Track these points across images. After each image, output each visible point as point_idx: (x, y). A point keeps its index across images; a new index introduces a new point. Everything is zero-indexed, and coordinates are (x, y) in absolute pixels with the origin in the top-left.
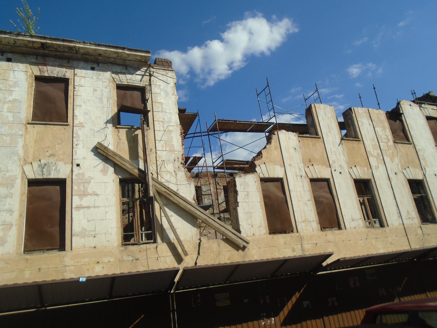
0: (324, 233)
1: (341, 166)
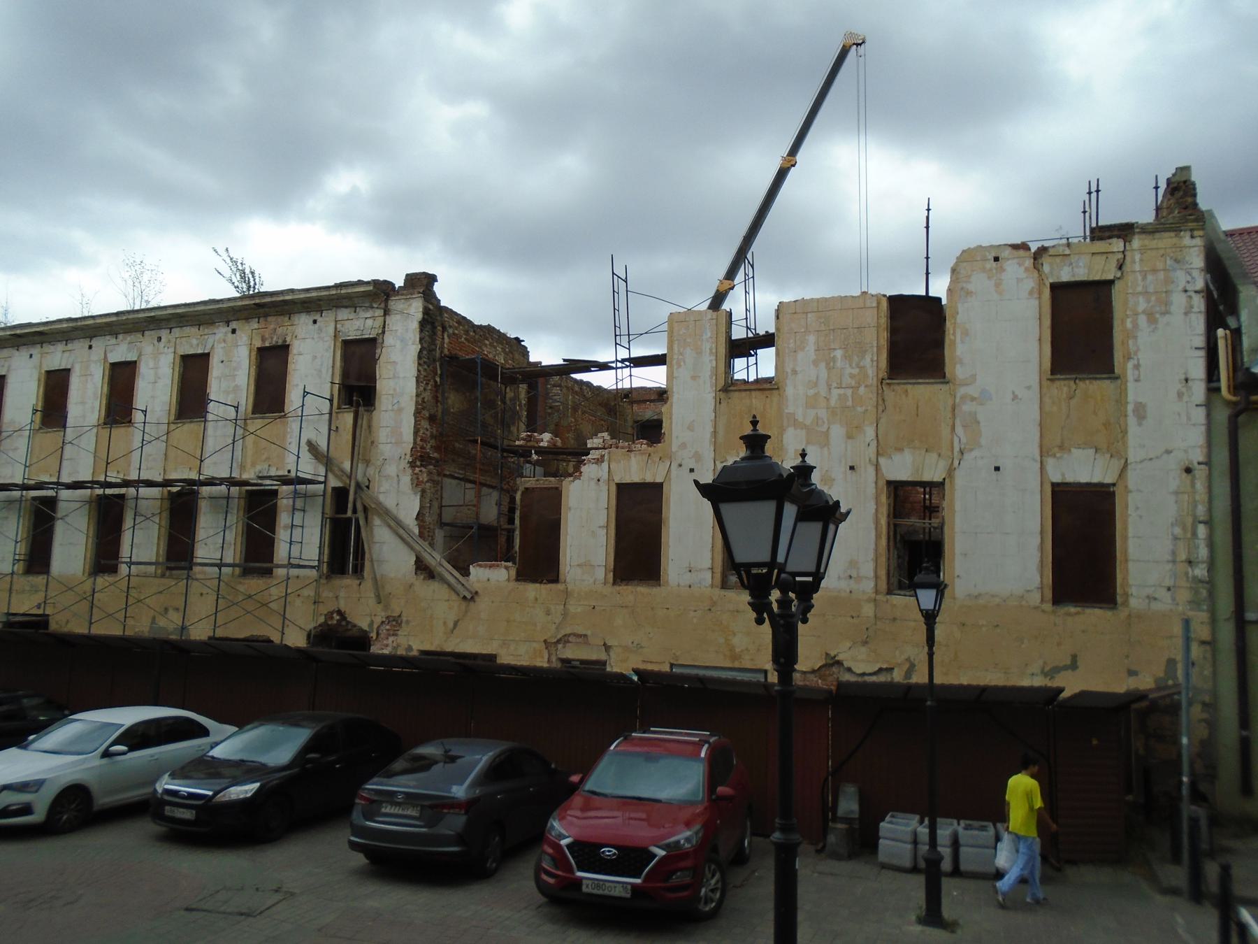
0: (617, 588)
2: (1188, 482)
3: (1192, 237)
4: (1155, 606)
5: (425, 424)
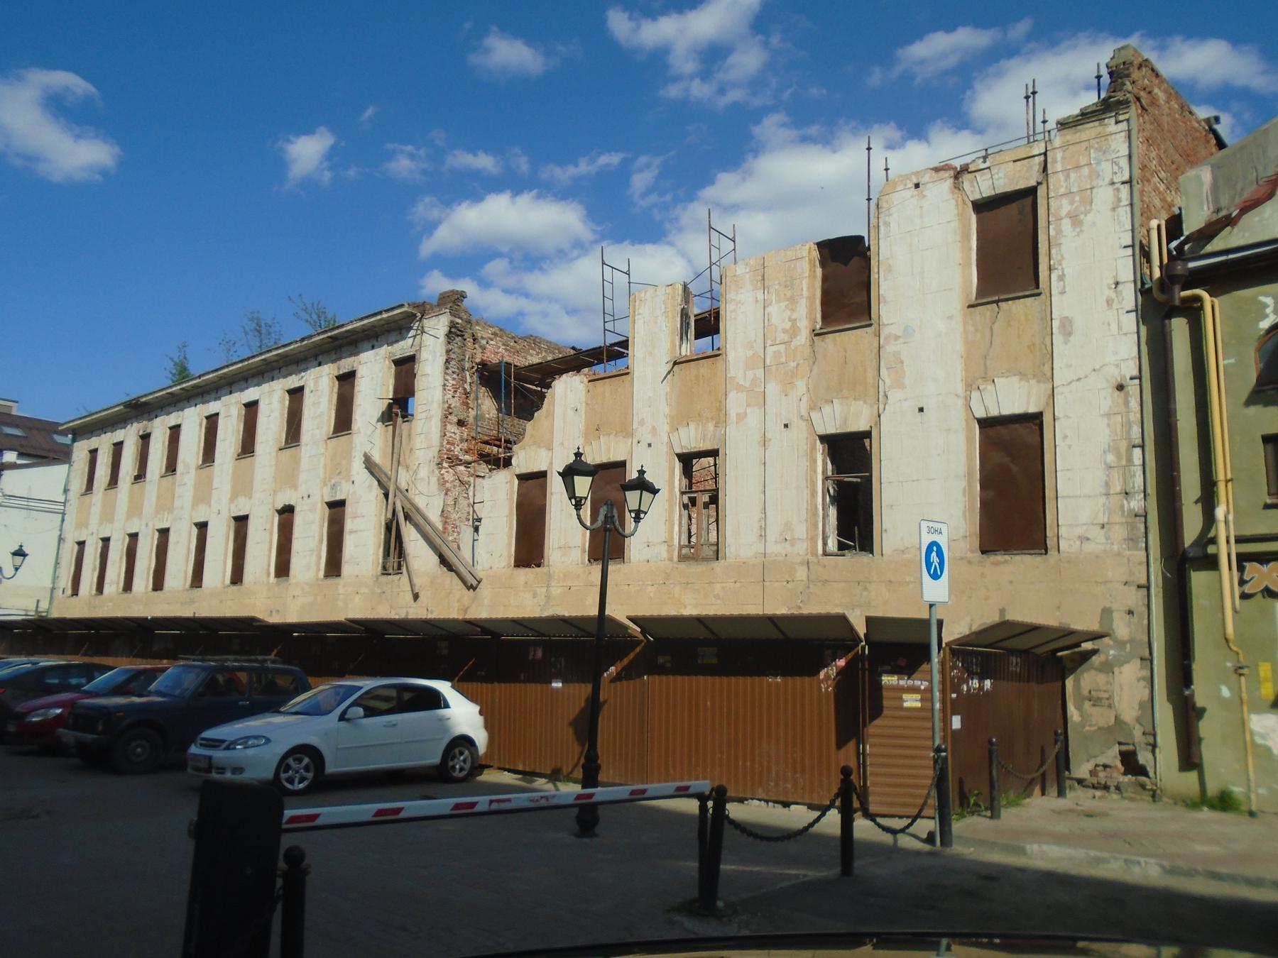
1: (654, 430)
2: (1121, 401)
3: (1117, 122)
4: (1089, 547)
5: (452, 428)
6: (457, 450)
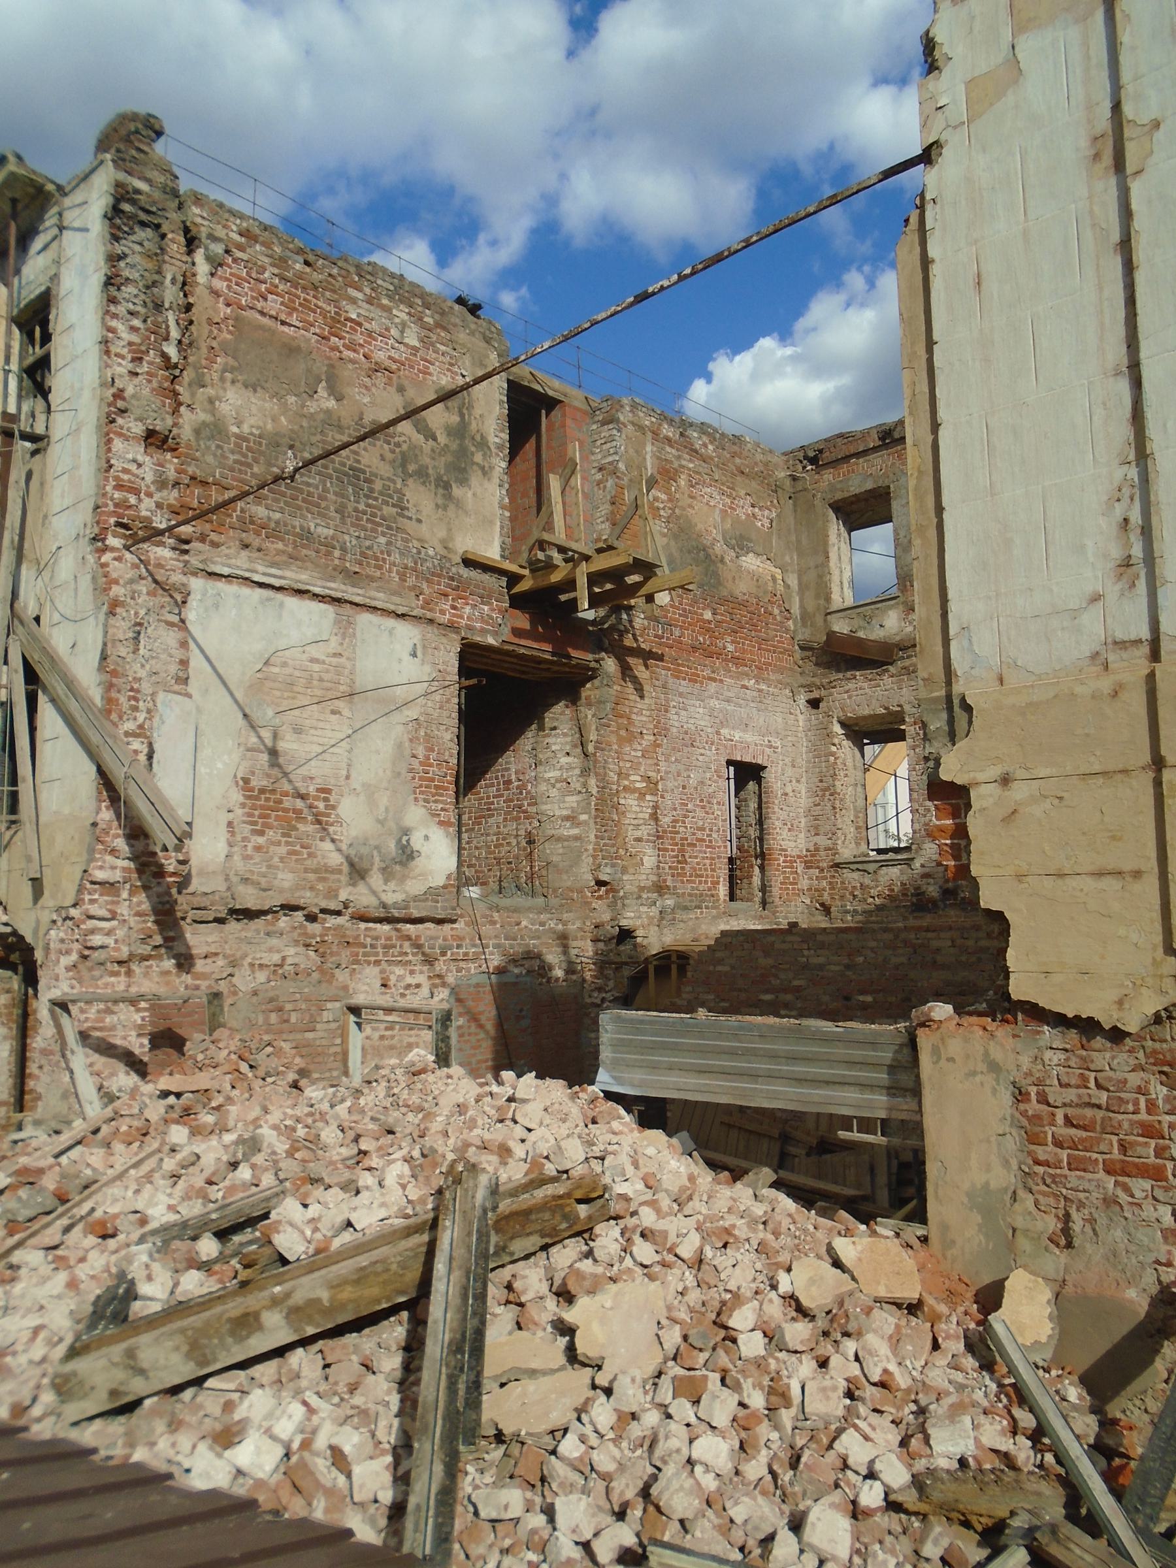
5: (128, 451)
6: (146, 507)
